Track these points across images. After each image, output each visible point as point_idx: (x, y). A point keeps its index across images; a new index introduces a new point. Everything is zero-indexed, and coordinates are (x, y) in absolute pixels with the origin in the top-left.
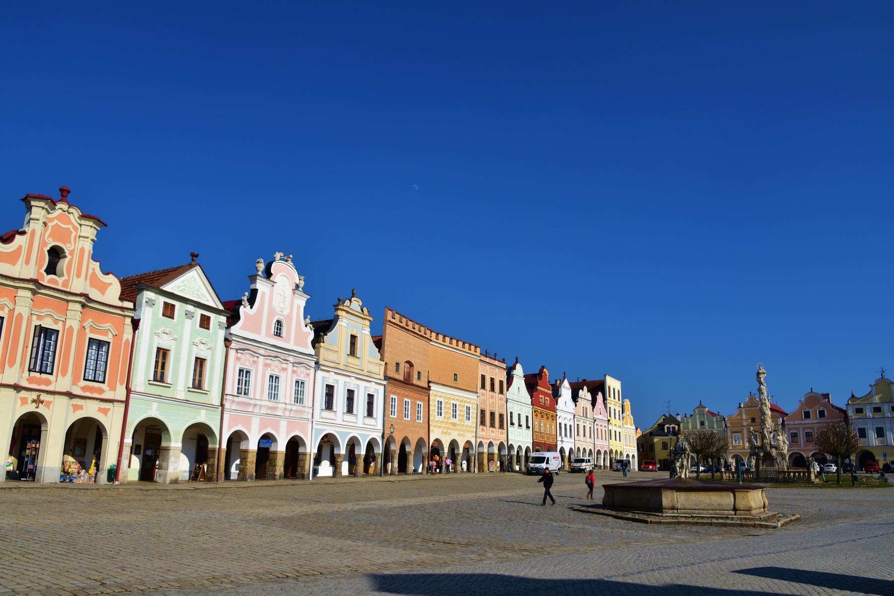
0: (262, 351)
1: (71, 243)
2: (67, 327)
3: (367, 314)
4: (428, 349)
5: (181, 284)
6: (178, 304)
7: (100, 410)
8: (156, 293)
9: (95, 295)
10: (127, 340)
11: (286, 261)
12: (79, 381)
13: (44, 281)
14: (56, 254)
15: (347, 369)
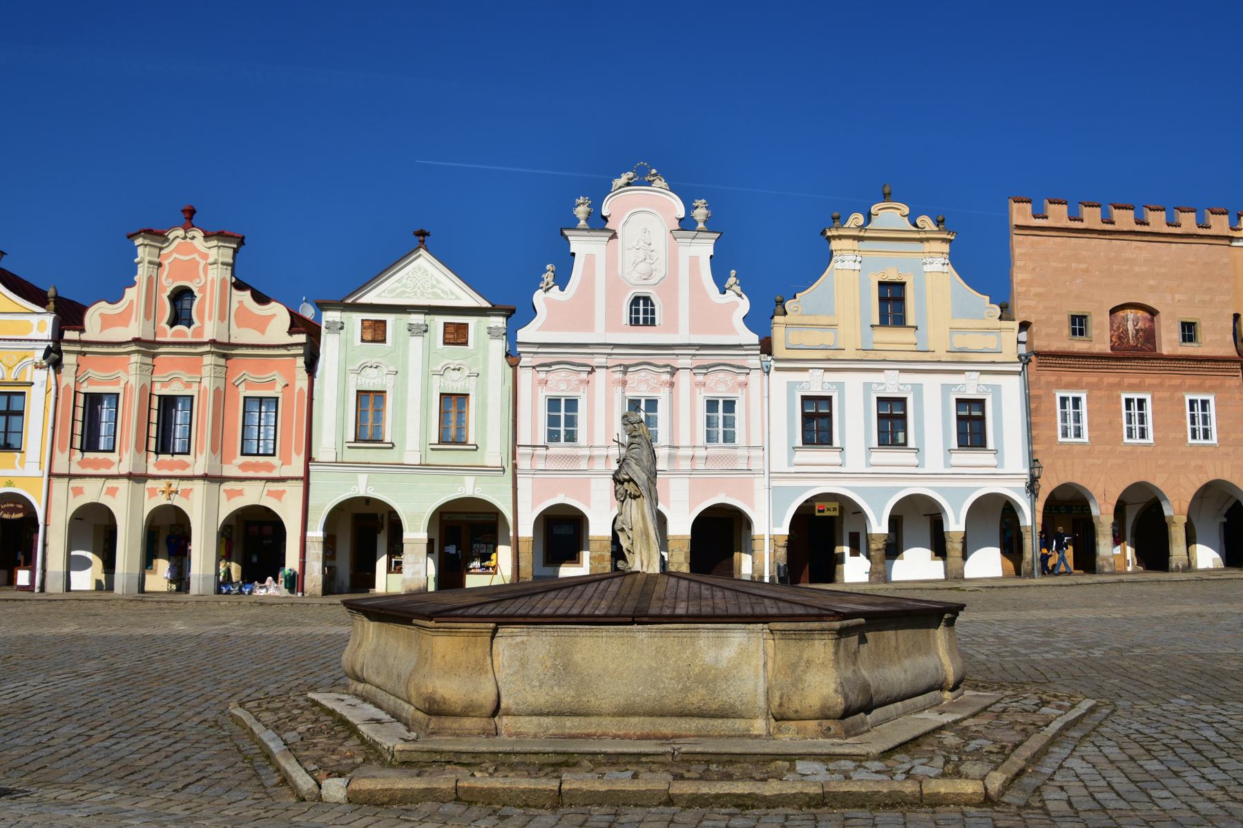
0: (600, 360)
1: (199, 277)
2: (202, 389)
3: (936, 229)
4: (1225, 260)
5: (397, 285)
6: (390, 318)
7: (270, 493)
8: (342, 311)
9: (242, 335)
10: (301, 389)
11: (650, 183)
12: (235, 458)
13: (165, 335)
14: (181, 296)
15: (871, 356)
